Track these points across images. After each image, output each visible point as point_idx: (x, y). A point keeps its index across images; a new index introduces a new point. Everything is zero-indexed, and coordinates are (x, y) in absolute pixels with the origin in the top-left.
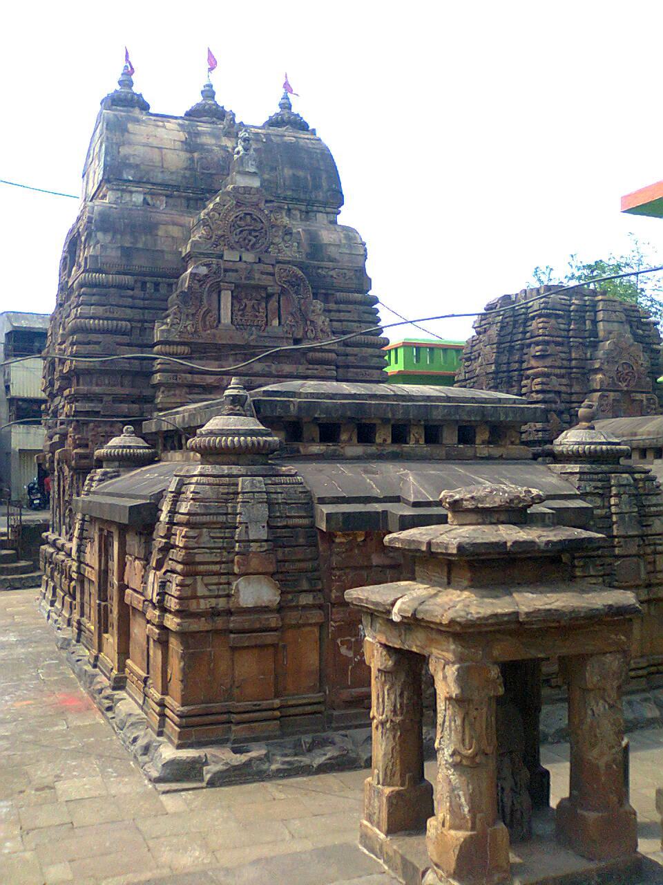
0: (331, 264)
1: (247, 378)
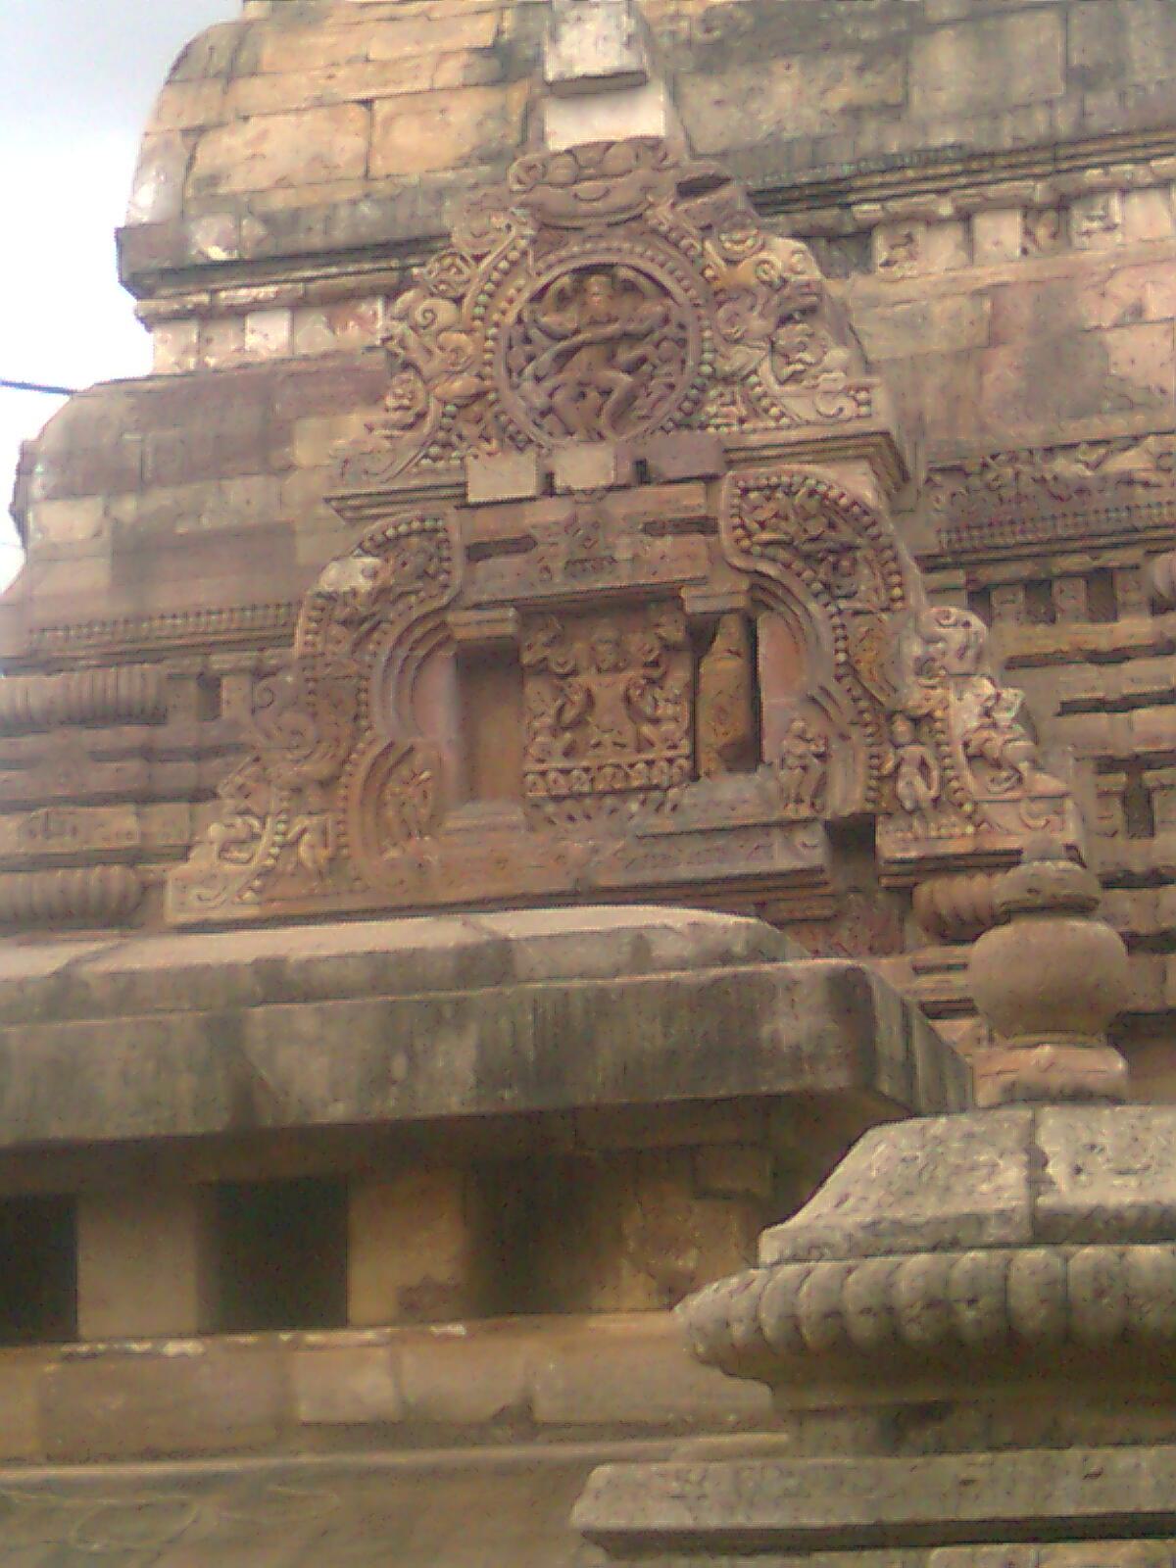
0: (1120, 425)
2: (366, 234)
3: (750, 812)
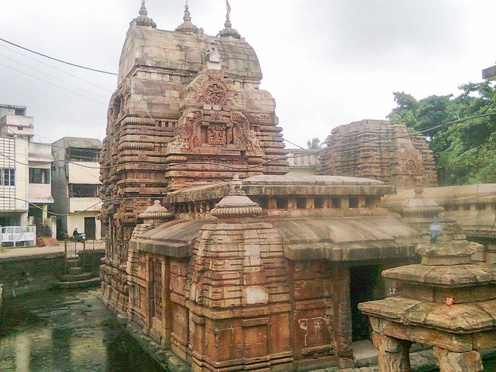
0: (257, 111)
1: (217, 173)
2: (168, 67)
3: (234, 149)
